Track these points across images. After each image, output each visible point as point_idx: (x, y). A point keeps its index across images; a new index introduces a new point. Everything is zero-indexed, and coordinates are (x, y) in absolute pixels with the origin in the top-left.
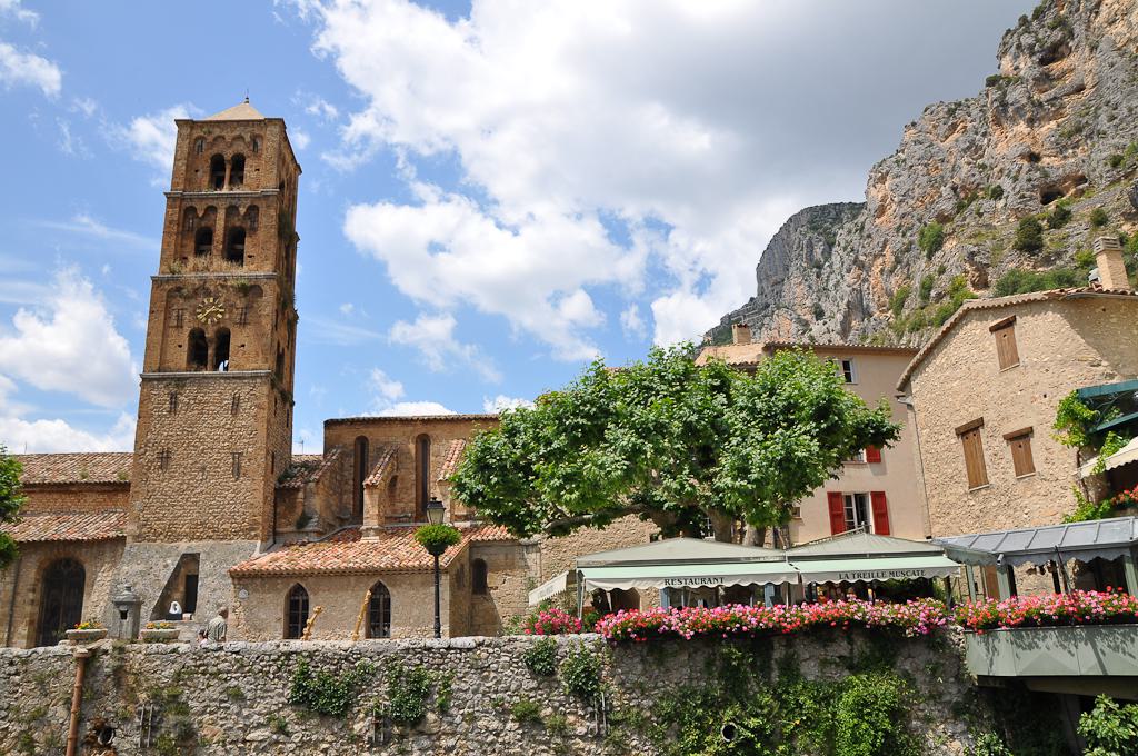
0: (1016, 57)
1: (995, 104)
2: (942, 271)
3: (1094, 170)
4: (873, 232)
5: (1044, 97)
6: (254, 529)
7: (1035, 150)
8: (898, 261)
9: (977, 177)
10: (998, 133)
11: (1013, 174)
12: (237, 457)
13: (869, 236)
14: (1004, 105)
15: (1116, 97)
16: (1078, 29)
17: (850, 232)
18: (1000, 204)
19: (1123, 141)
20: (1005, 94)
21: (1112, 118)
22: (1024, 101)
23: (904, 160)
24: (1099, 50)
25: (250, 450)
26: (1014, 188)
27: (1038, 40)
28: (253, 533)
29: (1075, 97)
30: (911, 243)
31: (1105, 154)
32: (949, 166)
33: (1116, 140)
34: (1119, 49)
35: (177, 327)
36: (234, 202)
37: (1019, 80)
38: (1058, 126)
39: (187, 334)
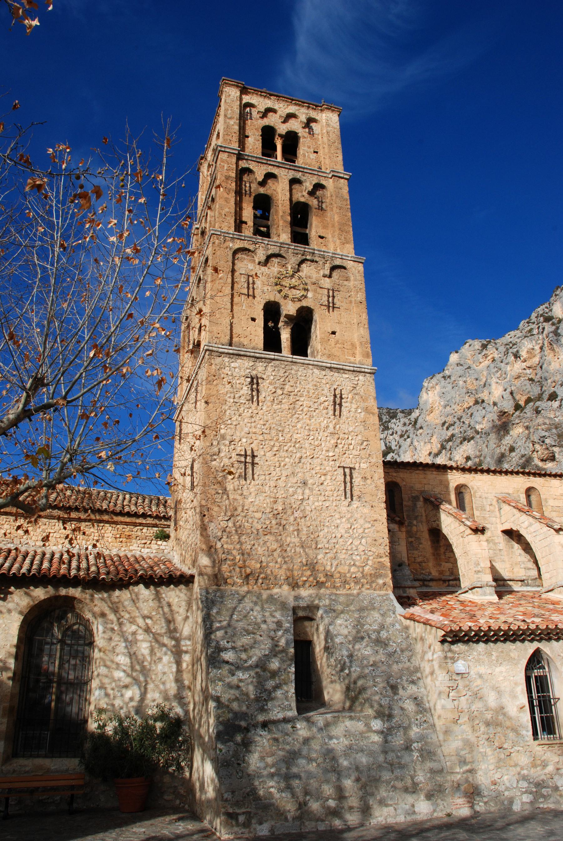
2: (512, 449)
4: (424, 425)
6: (380, 576)
8: (443, 447)
13: (421, 428)
17: (405, 424)
20: (558, 328)
23: (449, 377)
25: (363, 466)
28: (381, 581)
30: (453, 435)
32: (482, 383)
35: (248, 295)
36: (299, 175)
39: (262, 307)
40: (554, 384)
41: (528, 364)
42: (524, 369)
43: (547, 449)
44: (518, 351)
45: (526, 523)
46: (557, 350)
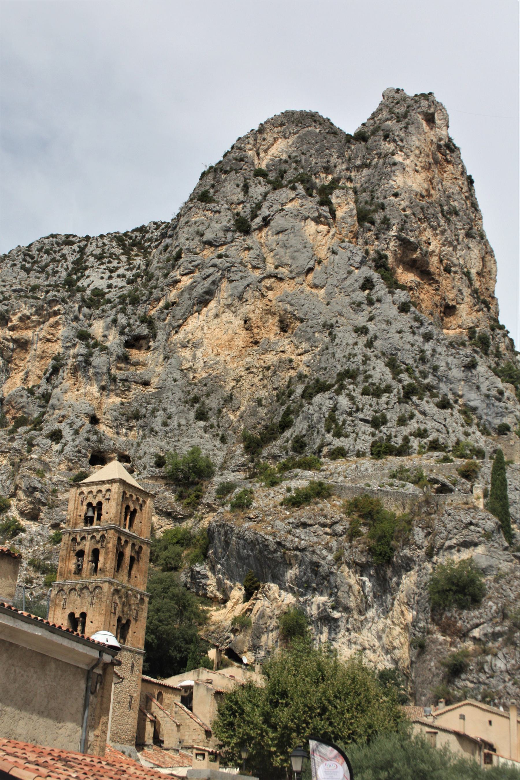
0: (108, 328)
1: (80, 358)
3: (140, 458)
5: (120, 375)
7: (99, 415)
9: (24, 399)
10: (71, 382)
11: (75, 427)
12: (131, 697)
14: (88, 363)
15: (172, 409)
16: (161, 335)
18: (57, 447)
19: (167, 447)
20: (91, 354)
21: (165, 424)
22: (105, 370)
24: (170, 361)
26: (73, 440)
27: (129, 325)
29: (141, 387)
31: (152, 450)
33: (163, 444)
34: (182, 370)
37: (104, 349)
38: (122, 404)
40: (61, 419)
41: (15, 335)
42: (7, 340)
43: (31, 503)
44: (7, 311)
45: (162, 715)
46: (80, 379)
